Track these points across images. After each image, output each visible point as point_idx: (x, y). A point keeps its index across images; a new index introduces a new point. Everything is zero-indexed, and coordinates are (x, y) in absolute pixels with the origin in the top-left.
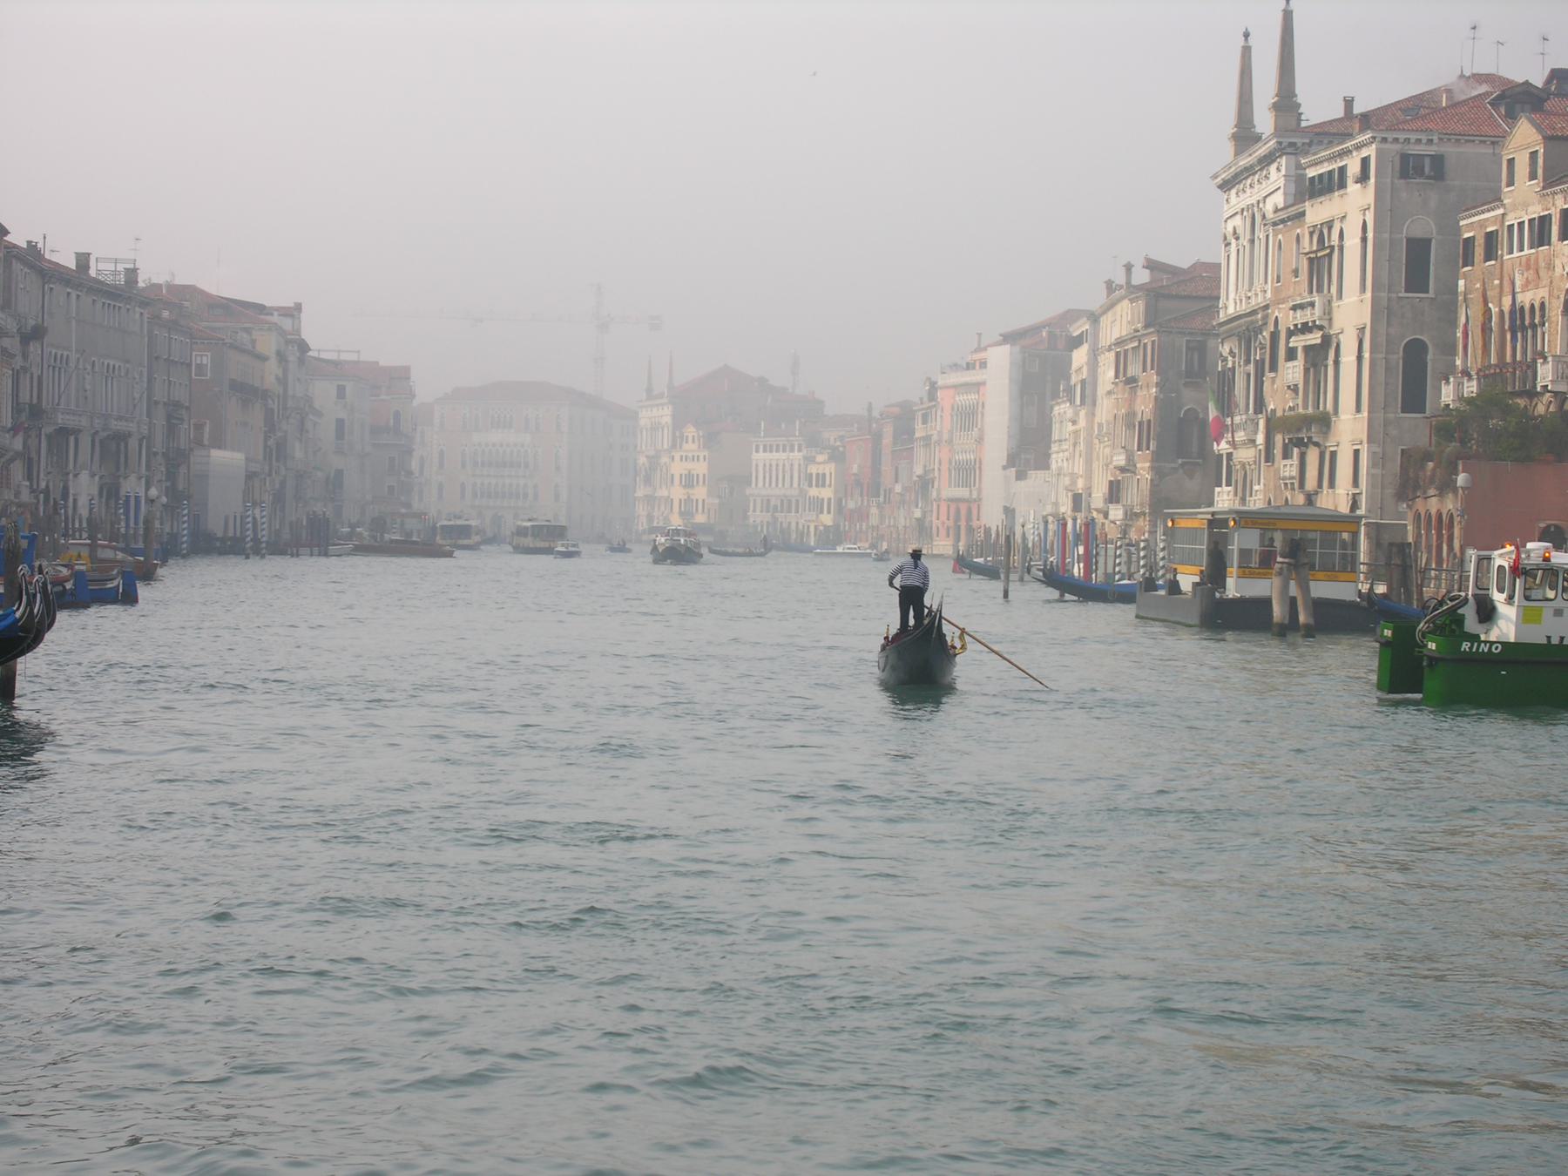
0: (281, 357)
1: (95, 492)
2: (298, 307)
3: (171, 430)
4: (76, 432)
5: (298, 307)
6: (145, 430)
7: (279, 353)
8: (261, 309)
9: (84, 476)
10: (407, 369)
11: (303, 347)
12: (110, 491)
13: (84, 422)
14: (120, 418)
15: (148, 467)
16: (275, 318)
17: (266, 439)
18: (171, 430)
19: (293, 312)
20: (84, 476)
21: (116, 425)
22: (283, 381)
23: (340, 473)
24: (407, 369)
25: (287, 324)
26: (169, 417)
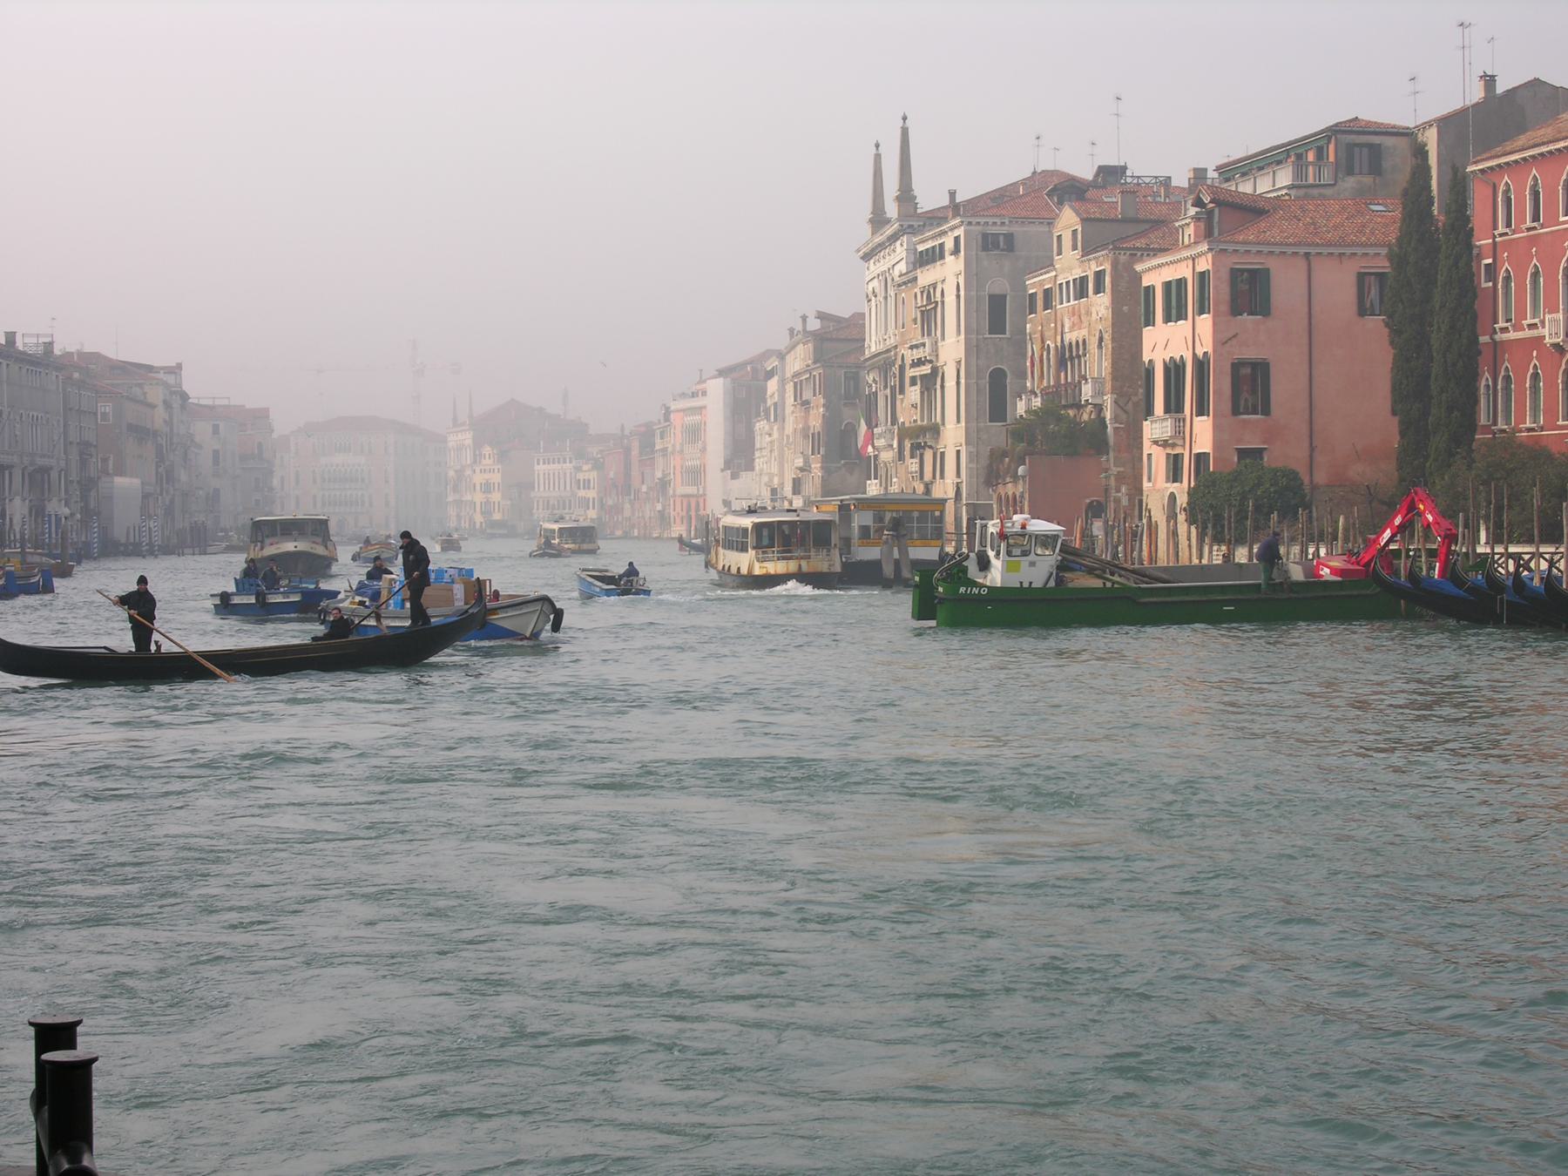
0: (167, 405)
1: (26, 512)
2: (179, 366)
3: (83, 463)
4: (10, 467)
5: (179, 366)
6: (63, 464)
7: (165, 402)
8: (150, 368)
9: (17, 501)
10: (267, 410)
11: (184, 397)
12: (38, 511)
13: (16, 459)
14: (43, 456)
15: (66, 491)
16: (161, 375)
17: (158, 467)
18: (83, 463)
19: (176, 370)
20: (17, 501)
21: (40, 462)
22: (169, 423)
23: (217, 491)
24: (267, 410)
25: (171, 379)
26: (81, 454)
